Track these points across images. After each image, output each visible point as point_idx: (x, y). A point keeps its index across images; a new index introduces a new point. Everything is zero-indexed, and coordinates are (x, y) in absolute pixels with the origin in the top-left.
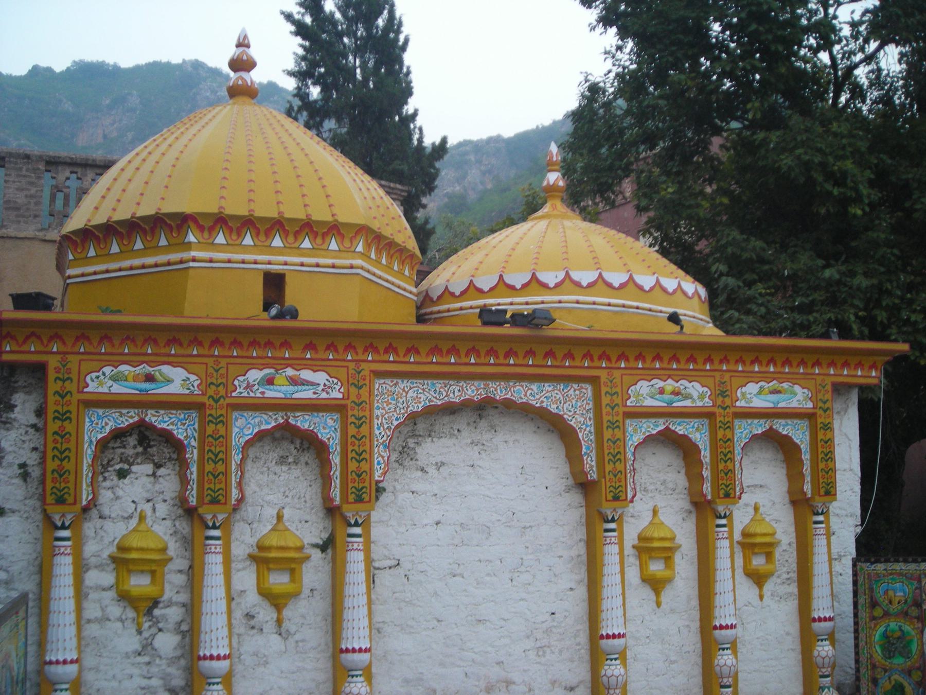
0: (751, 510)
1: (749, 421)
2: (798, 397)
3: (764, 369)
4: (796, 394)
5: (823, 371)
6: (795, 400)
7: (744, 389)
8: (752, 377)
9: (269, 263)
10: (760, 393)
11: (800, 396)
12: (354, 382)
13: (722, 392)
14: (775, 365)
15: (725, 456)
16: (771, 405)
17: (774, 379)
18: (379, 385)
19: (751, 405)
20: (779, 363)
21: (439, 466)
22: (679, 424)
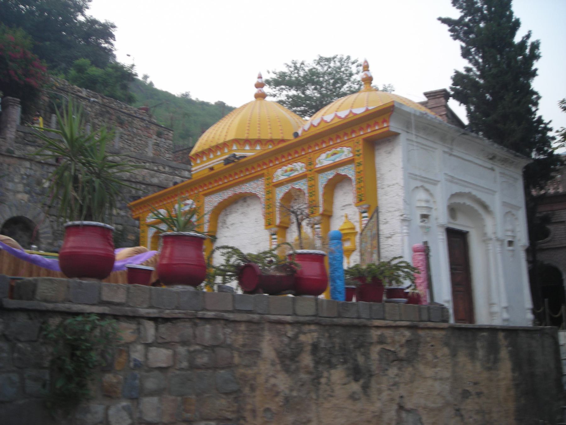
0: (344, 218)
2: (345, 153)
4: (343, 152)
5: (357, 135)
8: (322, 151)
10: (326, 158)
12: (197, 200)
13: (310, 163)
16: (331, 162)
17: (333, 148)
18: (207, 199)
19: (324, 165)
21: (233, 224)
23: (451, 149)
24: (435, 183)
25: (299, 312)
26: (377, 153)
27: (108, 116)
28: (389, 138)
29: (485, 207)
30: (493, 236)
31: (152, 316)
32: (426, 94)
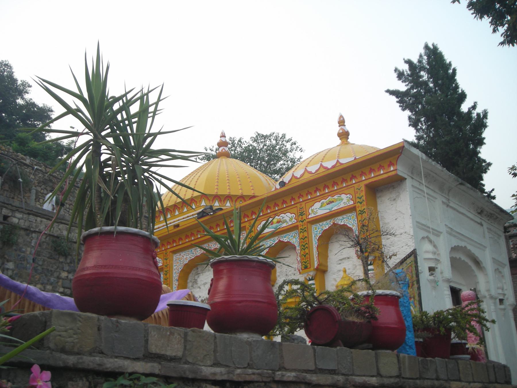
0: (342, 273)
1: (321, 224)
2: (344, 200)
3: (323, 192)
5: (357, 181)
6: (342, 203)
7: (313, 208)
9: (174, 222)
10: (321, 207)
11: (345, 200)
14: (328, 188)
15: (304, 246)
16: (329, 211)
17: (329, 196)
18: (175, 257)
19: (317, 215)
20: (330, 187)
22: (285, 237)
23: (449, 200)
24: (438, 234)
25: (383, 372)
26: (379, 201)
27: (51, 184)
28: (395, 183)
29: (477, 263)
30: (486, 294)
31: (219, 378)
32: (485, 114)
